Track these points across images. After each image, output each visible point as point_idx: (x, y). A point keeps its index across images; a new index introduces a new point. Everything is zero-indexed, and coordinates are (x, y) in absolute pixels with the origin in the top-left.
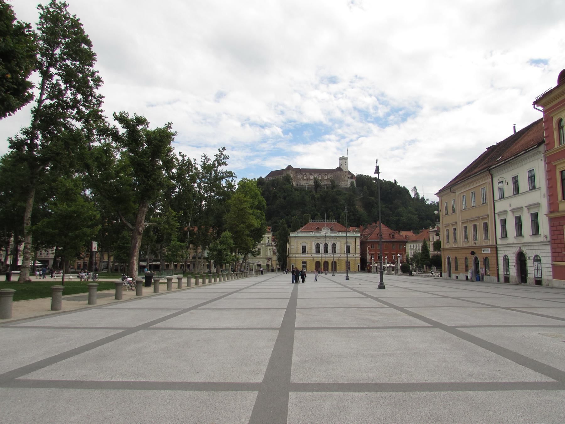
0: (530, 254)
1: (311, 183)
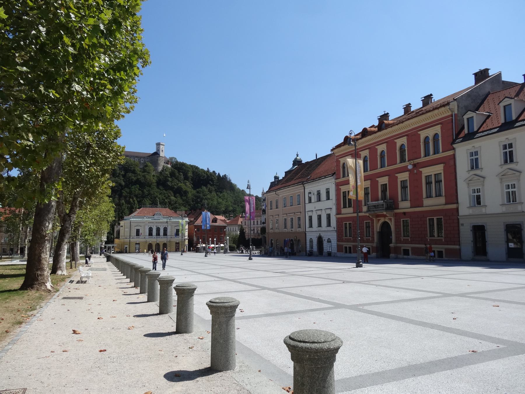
0: (325, 238)
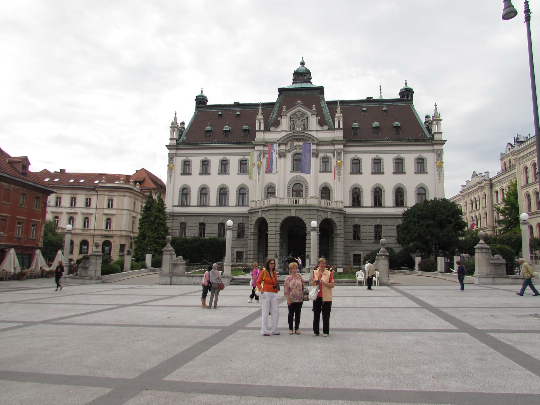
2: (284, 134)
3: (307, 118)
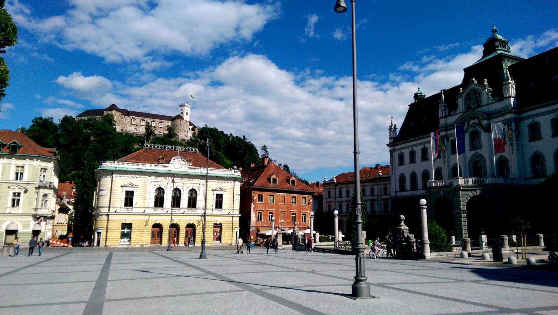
1: (142, 130)
2: (460, 115)
3: (479, 94)
